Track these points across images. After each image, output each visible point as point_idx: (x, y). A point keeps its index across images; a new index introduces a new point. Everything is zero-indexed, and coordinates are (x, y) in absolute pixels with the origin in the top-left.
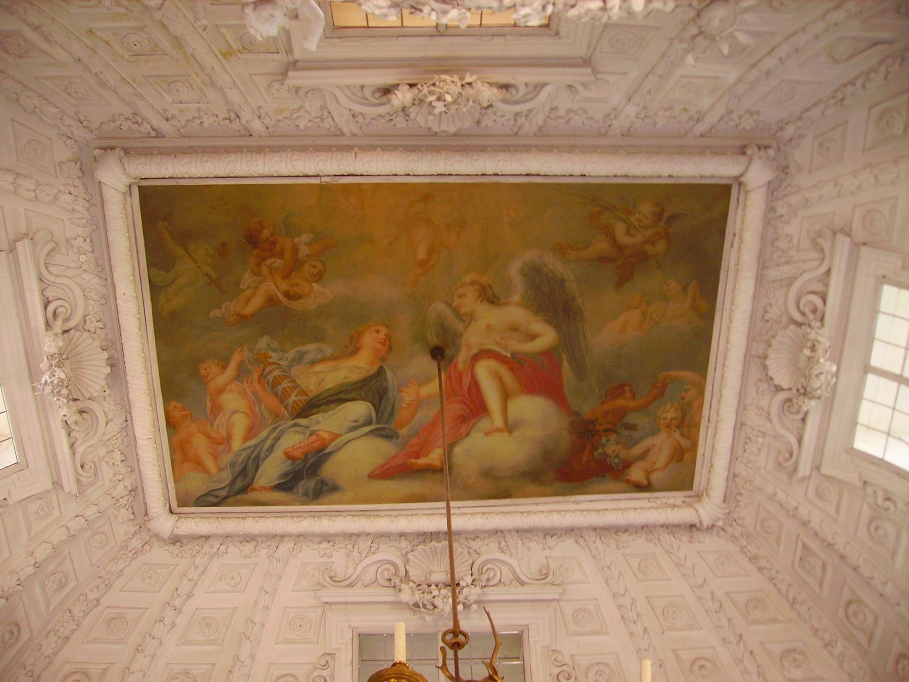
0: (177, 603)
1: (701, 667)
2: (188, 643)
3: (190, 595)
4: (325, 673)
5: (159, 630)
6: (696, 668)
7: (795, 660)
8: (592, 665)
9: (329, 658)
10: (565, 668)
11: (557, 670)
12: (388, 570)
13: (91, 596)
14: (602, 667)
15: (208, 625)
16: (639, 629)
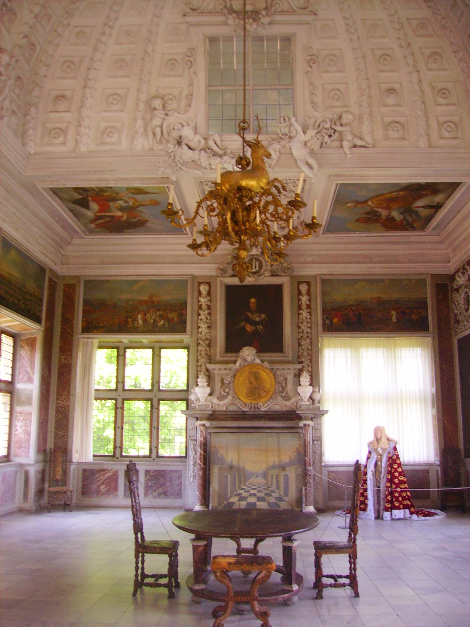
0: (111, 24)
1: (385, 59)
2: (120, 44)
3: (116, 19)
4: (191, 59)
5: (104, 39)
6: (382, 60)
7: (435, 59)
8: (327, 56)
9: (192, 51)
10: (313, 57)
11: (309, 58)
12: (221, 4)
13: (65, 22)
14: (333, 57)
15: (128, 34)
16: (354, 37)
